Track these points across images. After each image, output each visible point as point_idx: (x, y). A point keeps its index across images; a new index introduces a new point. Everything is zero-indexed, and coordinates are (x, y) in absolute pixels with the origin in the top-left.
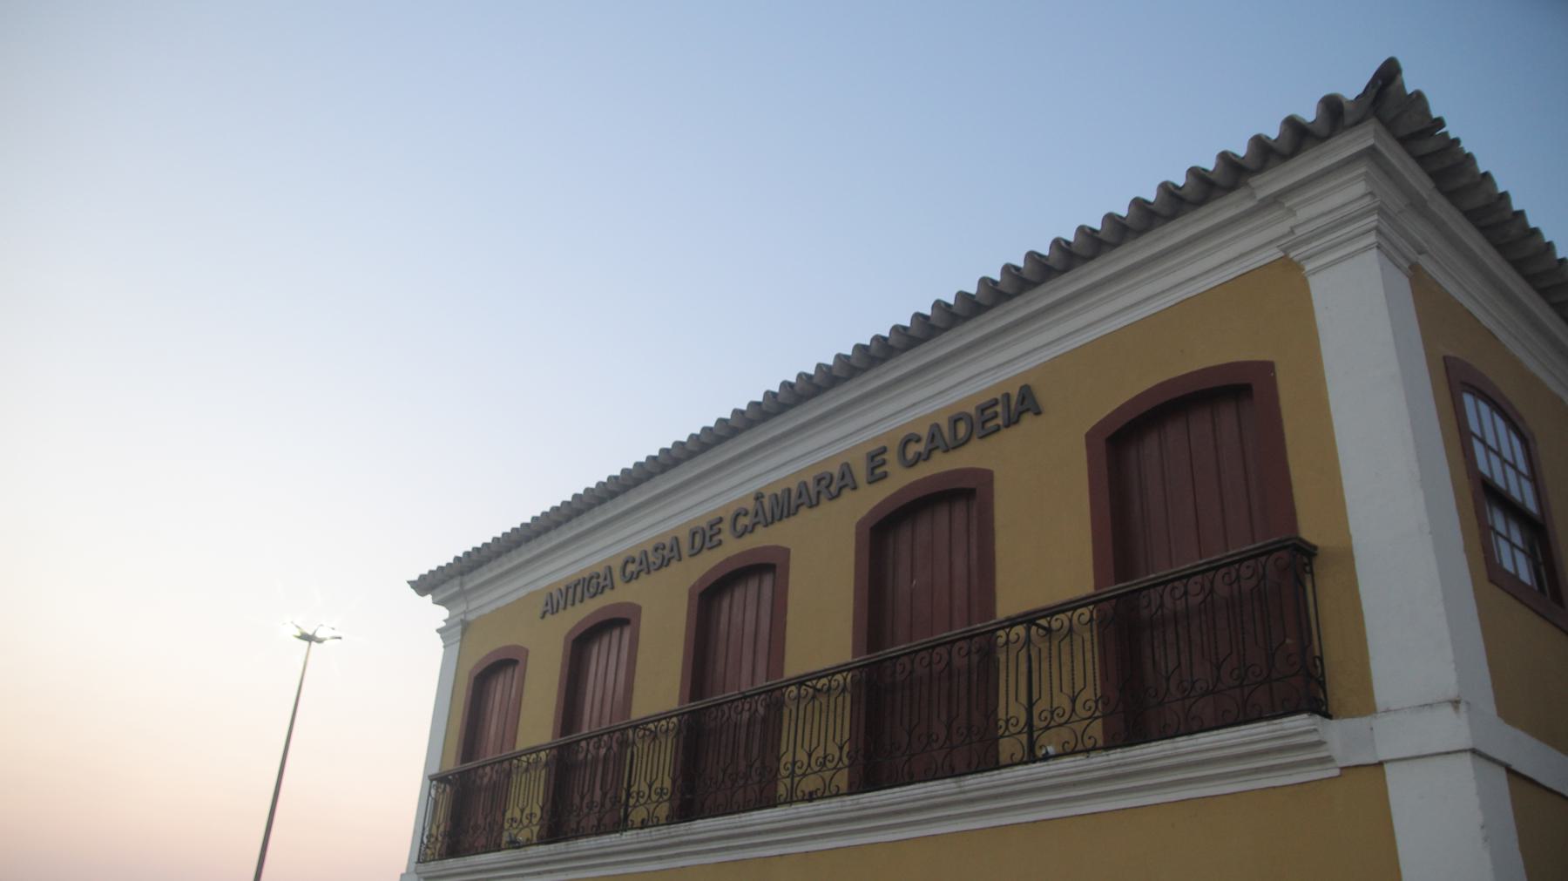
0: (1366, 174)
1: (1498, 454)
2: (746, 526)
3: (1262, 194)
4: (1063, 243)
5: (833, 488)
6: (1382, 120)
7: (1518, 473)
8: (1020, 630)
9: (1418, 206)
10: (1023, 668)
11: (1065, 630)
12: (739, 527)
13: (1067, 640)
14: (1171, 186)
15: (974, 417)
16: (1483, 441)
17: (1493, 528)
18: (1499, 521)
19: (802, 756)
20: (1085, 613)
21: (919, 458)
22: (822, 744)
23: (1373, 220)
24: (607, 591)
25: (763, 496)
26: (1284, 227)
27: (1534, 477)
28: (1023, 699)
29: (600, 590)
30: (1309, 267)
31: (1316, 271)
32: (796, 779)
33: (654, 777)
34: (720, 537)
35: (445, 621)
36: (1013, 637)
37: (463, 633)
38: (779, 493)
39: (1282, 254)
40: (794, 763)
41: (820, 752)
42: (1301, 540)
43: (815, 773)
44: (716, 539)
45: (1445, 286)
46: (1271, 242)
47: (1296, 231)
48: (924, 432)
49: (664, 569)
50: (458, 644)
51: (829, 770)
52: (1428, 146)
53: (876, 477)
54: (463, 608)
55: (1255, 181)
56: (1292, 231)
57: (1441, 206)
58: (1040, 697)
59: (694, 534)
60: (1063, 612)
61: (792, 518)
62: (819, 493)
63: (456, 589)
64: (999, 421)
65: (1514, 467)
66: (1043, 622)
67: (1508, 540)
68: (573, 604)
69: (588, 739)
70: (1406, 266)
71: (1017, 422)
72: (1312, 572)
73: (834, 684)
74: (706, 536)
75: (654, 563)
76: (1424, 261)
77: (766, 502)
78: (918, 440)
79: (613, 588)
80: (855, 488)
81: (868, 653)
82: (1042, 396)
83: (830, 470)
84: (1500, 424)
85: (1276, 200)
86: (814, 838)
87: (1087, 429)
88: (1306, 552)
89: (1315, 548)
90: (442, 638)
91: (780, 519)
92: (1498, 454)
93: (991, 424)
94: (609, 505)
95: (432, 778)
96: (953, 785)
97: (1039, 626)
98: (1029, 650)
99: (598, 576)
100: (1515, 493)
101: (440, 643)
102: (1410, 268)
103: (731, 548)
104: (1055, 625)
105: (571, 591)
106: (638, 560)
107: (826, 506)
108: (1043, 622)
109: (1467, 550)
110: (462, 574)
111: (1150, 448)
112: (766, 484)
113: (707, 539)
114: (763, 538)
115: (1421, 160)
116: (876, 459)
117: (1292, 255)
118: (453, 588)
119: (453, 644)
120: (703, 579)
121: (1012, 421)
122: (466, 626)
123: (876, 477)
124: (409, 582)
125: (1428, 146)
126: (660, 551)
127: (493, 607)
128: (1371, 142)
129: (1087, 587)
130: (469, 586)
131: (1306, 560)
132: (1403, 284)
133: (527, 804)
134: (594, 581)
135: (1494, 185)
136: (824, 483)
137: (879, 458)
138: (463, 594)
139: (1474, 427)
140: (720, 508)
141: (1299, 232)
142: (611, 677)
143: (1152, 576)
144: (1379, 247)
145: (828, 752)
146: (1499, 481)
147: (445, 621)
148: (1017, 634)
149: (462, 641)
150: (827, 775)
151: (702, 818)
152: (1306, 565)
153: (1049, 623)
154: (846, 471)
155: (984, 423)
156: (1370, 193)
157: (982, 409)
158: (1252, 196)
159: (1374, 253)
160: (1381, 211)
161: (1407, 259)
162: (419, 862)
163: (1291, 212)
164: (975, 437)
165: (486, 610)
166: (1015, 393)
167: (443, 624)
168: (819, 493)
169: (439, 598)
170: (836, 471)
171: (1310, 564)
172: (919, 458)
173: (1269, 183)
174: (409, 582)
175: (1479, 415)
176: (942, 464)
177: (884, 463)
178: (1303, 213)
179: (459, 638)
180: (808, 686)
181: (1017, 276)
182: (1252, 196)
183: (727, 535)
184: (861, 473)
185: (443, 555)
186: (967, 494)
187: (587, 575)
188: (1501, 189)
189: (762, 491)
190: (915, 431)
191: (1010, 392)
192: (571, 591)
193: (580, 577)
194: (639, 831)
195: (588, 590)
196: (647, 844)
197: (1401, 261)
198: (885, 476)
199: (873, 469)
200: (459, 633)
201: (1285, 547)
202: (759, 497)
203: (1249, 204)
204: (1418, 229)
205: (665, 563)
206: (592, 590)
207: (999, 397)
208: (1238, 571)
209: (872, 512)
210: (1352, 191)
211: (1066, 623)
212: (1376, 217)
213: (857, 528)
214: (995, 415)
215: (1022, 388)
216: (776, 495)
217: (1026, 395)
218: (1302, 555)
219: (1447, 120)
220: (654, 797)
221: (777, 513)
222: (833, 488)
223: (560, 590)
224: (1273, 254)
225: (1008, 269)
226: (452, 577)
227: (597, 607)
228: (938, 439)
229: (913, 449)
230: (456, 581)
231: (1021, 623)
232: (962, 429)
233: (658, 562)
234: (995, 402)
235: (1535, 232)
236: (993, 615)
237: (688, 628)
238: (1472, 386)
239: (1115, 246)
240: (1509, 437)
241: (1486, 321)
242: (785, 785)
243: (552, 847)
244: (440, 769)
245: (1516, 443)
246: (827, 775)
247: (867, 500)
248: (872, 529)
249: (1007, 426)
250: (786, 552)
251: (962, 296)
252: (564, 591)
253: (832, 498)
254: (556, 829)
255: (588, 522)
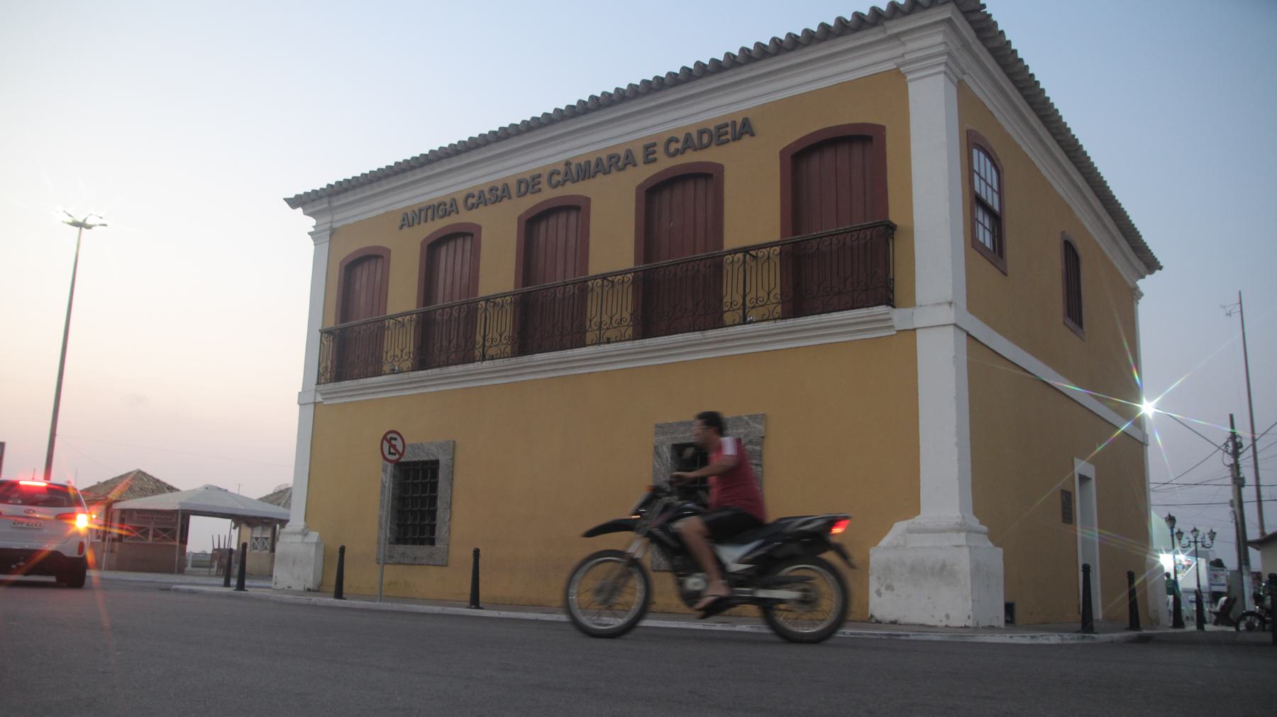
0: (944, 31)
1: (985, 181)
2: (559, 182)
3: (890, 32)
4: (777, 40)
5: (620, 164)
6: (956, 4)
7: (993, 190)
8: (740, 255)
9: (966, 46)
10: (741, 277)
11: (766, 257)
12: (554, 182)
13: (766, 264)
14: (843, 20)
15: (713, 134)
16: (979, 174)
17: (977, 219)
18: (980, 215)
19: (606, 318)
20: (778, 249)
21: (677, 152)
22: (619, 312)
23: (944, 58)
24: (453, 214)
25: (571, 164)
26: (899, 51)
27: (1000, 192)
28: (741, 292)
29: (447, 214)
30: (909, 77)
31: (912, 80)
32: (602, 332)
33: (503, 329)
34: (540, 186)
35: (314, 227)
36: (736, 259)
37: (331, 235)
38: (583, 164)
39: (895, 67)
40: (601, 323)
41: (617, 317)
42: (891, 223)
43: (615, 328)
44: (537, 187)
45: (972, 88)
46: (892, 59)
47: (906, 56)
48: (682, 137)
49: (497, 204)
50: (328, 243)
51: (623, 326)
52: (976, 17)
53: (649, 160)
54: (328, 219)
55: (887, 24)
56: (903, 55)
57: (978, 47)
58: (750, 292)
59: (520, 182)
60: (765, 248)
61: (592, 180)
62: (611, 166)
63: (326, 205)
64: (729, 137)
65: (991, 187)
66: (753, 253)
67: (983, 225)
68: (426, 221)
69: (443, 309)
70: (956, 81)
71: (739, 139)
72: (893, 239)
73: (626, 279)
74: (529, 184)
75: (490, 199)
76: (966, 78)
77: (573, 168)
78: (677, 141)
79: (458, 213)
80: (635, 165)
81: (645, 263)
82: (757, 126)
83: (618, 152)
84: (988, 163)
85: (897, 36)
86: (622, 361)
87: (781, 148)
88: (891, 228)
89: (896, 226)
90: (312, 238)
91: (583, 179)
92: (985, 181)
93: (723, 138)
94: (455, 159)
95: (323, 332)
96: (700, 335)
97: (751, 255)
98: (744, 266)
99: (445, 205)
100: (990, 202)
101: (312, 242)
102: (958, 82)
103: (548, 194)
104: (760, 254)
105: (423, 213)
106: (476, 194)
107: (615, 175)
108: (753, 253)
109: (965, 233)
110: (330, 195)
111: (814, 161)
112: (572, 156)
113: (530, 187)
114: (571, 190)
115: (971, 23)
116: (649, 149)
117: (901, 69)
118: (324, 205)
119: (325, 242)
120: (527, 212)
121: (737, 138)
122: (333, 232)
123: (649, 160)
124: (285, 199)
125: (976, 17)
126: (494, 191)
127: (356, 219)
128: (949, 16)
129: (776, 237)
130: (335, 204)
131: (891, 232)
132: (954, 91)
133: (391, 349)
134: (442, 207)
135: (1005, 37)
136: (613, 160)
137: (651, 149)
138: (330, 210)
139: (976, 168)
140: (539, 168)
141: (908, 57)
142: (458, 268)
143: (815, 233)
144: (945, 73)
145: (603, 320)
146: (984, 196)
147: (314, 227)
148: (738, 258)
149: (330, 241)
150: (623, 330)
151: (540, 353)
152: (890, 234)
153: (757, 254)
154: (629, 154)
155: (719, 136)
156: (945, 43)
157: (719, 128)
158: (885, 31)
159: (942, 76)
160: (949, 54)
161: (957, 77)
162: (318, 383)
163: (903, 44)
164: (713, 144)
165: (351, 221)
166: (739, 121)
167: (313, 230)
168: (611, 166)
169: (311, 210)
170: (622, 154)
171: (893, 234)
172: (677, 152)
173: (895, 27)
174: (285, 199)
175: (980, 160)
176: (691, 157)
177: (654, 152)
178: (911, 46)
179: (328, 239)
180: (609, 281)
181: (749, 56)
182: (885, 31)
183: (544, 185)
184: (639, 156)
185: (319, 182)
186: (707, 176)
187: (436, 203)
188: (1007, 39)
189: (571, 161)
190: (676, 136)
191: (736, 120)
192: (423, 213)
193: (431, 204)
194: (491, 361)
195: (438, 213)
196: (501, 368)
197: (953, 78)
198: (655, 160)
199: (647, 155)
200: (327, 236)
201: (882, 225)
202: (568, 164)
203: (882, 36)
204: (964, 60)
205: (498, 199)
206: (440, 213)
207: (729, 123)
208: (858, 234)
209: (646, 181)
210: (935, 40)
211: (766, 253)
212: (946, 57)
213: (636, 189)
214: (726, 133)
215: (743, 119)
216: (580, 164)
217: (746, 122)
218: (889, 229)
219: (987, 6)
220: (504, 342)
221: (581, 175)
222: (620, 164)
223: (414, 211)
224: (890, 66)
225: (743, 50)
226: (321, 197)
227: (444, 225)
228: (689, 143)
229: (673, 147)
230: (325, 200)
231: (741, 252)
232: (705, 139)
233: (493, 199)
234: (727, 125)
235: (1021, 60)
236: (722, 247)
237: (518, 242)
238: (979, 145)
239: (806, 45)
240: (991, 170)
241: (991, 107)
242: (739, 314)
243: (421, 373)
244: (323, 326)
245: (994, 173)
246: (623, 330)
247: (643, 173)
248: (646, 191)
249: (734, 139)
250: (588, 200)
251: (713, 61)
252: (417, 213)
253: (620, 170)
254: (424, 360)
255: (437, 169)
